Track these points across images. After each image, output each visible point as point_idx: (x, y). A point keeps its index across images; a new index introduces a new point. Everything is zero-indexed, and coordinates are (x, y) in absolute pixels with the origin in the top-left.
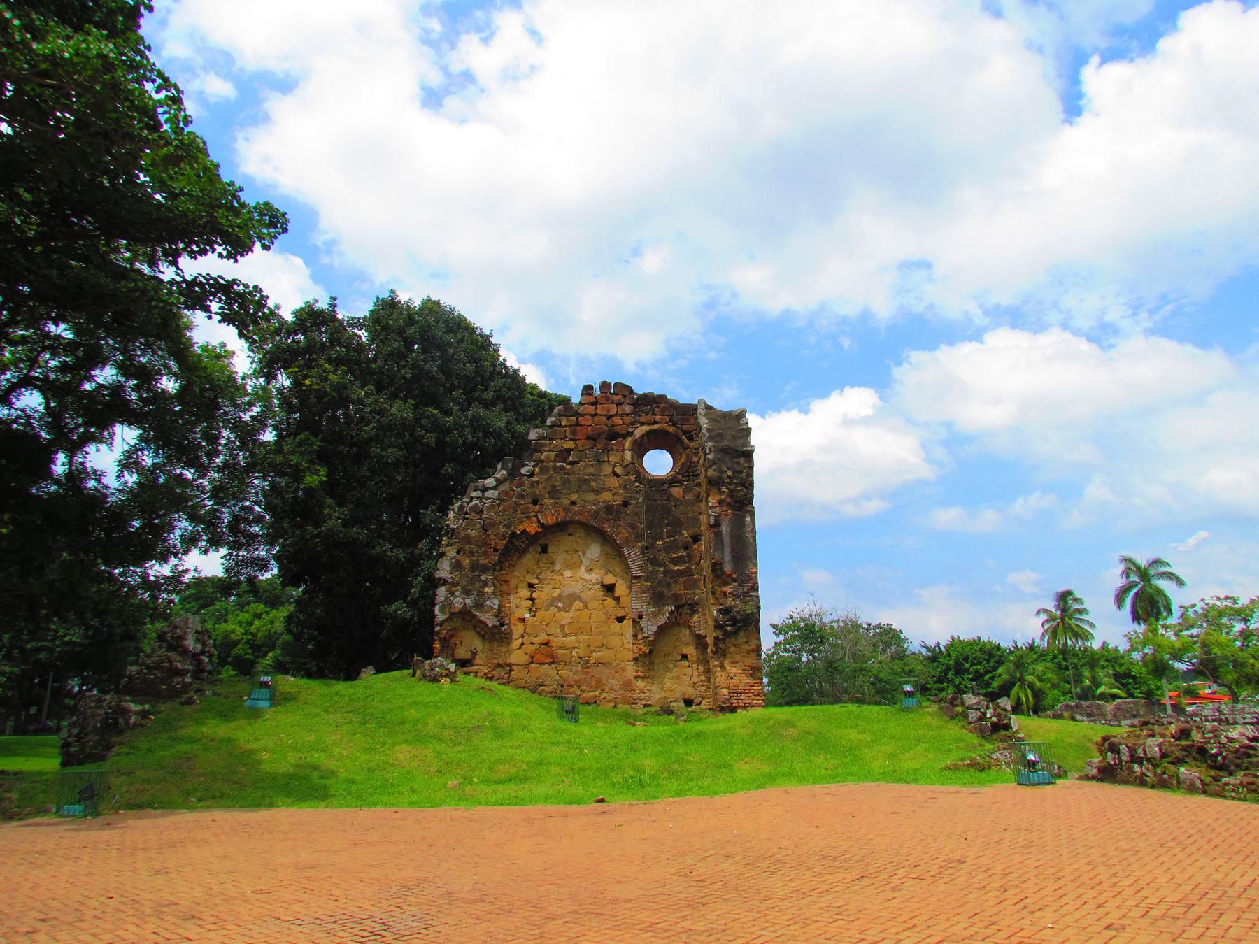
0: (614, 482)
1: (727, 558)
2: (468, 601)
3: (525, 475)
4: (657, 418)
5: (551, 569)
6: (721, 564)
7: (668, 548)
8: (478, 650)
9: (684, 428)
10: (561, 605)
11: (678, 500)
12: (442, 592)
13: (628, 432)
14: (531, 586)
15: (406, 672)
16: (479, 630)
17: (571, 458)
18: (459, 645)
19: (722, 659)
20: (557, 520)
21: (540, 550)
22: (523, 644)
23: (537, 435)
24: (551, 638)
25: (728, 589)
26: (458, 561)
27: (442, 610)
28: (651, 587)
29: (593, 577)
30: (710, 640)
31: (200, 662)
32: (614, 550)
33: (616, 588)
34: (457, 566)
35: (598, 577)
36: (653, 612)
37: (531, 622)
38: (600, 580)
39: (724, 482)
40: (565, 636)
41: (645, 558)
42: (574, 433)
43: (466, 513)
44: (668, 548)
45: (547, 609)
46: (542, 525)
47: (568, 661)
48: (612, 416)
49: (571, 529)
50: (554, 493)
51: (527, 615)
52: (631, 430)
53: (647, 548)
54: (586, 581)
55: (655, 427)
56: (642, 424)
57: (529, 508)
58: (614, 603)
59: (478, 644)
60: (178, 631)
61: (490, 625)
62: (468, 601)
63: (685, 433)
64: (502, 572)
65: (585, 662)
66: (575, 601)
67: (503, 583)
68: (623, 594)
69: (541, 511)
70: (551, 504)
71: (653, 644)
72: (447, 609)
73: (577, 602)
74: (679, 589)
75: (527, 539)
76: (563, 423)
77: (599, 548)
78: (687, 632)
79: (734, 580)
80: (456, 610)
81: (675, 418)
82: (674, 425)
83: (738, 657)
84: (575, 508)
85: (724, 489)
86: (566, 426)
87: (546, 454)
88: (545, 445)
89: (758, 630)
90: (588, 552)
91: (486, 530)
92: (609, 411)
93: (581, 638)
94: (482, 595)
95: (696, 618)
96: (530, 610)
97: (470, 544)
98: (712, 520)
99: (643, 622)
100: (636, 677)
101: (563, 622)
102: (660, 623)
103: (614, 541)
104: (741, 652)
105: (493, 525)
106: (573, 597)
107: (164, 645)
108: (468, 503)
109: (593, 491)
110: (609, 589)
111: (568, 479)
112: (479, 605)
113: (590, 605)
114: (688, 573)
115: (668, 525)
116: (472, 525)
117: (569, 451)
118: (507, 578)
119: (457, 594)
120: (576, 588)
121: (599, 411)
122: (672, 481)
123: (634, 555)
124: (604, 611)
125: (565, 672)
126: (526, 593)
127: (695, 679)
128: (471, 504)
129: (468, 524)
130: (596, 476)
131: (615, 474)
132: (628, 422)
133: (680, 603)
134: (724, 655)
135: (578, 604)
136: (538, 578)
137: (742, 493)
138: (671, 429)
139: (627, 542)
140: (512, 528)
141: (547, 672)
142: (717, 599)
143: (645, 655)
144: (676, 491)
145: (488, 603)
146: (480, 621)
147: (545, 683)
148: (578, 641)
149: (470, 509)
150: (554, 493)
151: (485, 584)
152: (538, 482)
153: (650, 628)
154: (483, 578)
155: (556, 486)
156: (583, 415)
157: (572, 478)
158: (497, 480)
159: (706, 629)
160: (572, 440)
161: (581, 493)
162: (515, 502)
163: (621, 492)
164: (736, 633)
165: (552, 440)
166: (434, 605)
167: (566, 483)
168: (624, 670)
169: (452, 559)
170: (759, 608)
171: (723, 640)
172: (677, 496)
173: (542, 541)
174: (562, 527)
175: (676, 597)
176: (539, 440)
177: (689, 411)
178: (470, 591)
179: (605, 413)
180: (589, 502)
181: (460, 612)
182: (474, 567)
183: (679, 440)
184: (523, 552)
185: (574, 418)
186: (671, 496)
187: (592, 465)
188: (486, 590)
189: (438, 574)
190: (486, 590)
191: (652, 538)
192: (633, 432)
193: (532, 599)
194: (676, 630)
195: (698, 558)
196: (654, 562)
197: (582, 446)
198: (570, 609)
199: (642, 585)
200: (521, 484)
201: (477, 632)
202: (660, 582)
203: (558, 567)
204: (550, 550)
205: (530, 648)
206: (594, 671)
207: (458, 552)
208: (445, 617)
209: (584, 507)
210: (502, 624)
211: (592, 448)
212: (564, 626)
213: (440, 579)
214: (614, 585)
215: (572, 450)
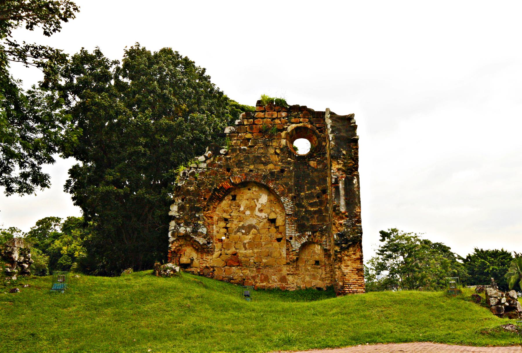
0: (276, 158)
1: (342, 202)
2: (188, 229)
3: (223, 154)
4: (301, 120)
5: (238, 210)
6: (339, 206)
8: (194, 258)
10: (244, 231)
12: (173, 224)
13: (284, 128)
14: (226, 220)
15: (150, 271)
16: (195, 246)
17: (250, 144)
18: (183, 255)
19: (340, 264)
20: (241, 180)
21: (231, 198)
22: (221, 255)
23: (230, 130)
24: (238, 251)
25: (342, 221)
26: (182, 205)
27: (173, 235)
28: (298, 220)
29: (263, 215)
30: (332, 252)
31: (23, 267)
33: (277, 221)
34: (181, 208)
35: (266, 215)
36: (298, 236)
37: (225, 241)
38: (267, 217)
39: (340, 158)
41: (294, 203)
42: (251, 129)
43: (187, 177)
45: (236, 233)
46: (233, 184)
47: (248, 265)
49: (250, 187)
50: (239, 164)
51: (224, 238)
52: (286, 127)
53: (295, 197)
54: (259, 217)
55: (301, 125)
56: (293, 123)
57: (224, 173)
58: (275, 230)
59: (194, 255)
60: (8, 248)
61: (201, 243)
63: (318, 128)
64: (209, 212)
66: (252, 229)
67: (209, 218)
68: (281, 224)
69: (231, 175)
70: (238, 171)
71: (298, 254)
72: (176, 234)
74: (314, 222)
75: (223, 191)
76: (245, 123)
77: (267, 197)
79: (347, 216)
80: (181, 235)
81: (312, 119)
82: (311, 124)
83: (349, 263)
85: (340, 162)
86: (247, 125)
87: (235, 141)
88: (235, 136)
89: (361, 247)
90: (260, 200)
91: (199, 187)
92: (272, 115)
93: (256, 251)
95: (324, 238)
96: (225, 234)
97: (190, 195)
98: (333, 180)
99: (293, 242)
100: (288, 274)
101: (245, 242)
102: (302, 242)
103: (276, 193)
104: (351, 260)
105: (203, 183)
106: (251, 227)
108: (188, 171)
111: (248, 156)
112: (195, 232)
113: (261, 232)
114: (320, 212)
115: (307, 183)
116: (190, 183)
117: (249, 140)
118: (212, 215)
119: (182, 225)
120: (254, 222)
121: (266, 116)
122: (310, 156)
123: (287, 201)
124: (269, 235)
125: (247, 272)
126: (222, 224)
127: (323, 276)
128: (191, 171)
129: (188, 183)
130: (265, 156)
131: (276, 153)
132: (284, 122)
133: (315, 230)
135: (254, 231)
136: (230, 215)
137: (351, 164)
138: (309, 126)
139: (283, 194)
140: (215, 186)
141: (236, 272)
143: (294, 261)
144: (312, 163)
145: (200, 230)
146: (195, 241)
147: (234, 278)
148: (254, 253)
149: (189, 175)
151: (199, 219)
152: (230, 158)
153: (296, 245)
154: (197, 215)
155: (241, 161)
156: (257, 118)
159: (330, 245)
160: (250, 133)
161: (256, 164)
162: (217, 170)
163: (279, 163)
164: (347, 248)
165: (238, 133)
166: (168, 231)
167: (247, 158)
168: (281, 270)
169: (179, 204)
170: (361, 233)
171: (340, 252)
172: (313, 166)
173: (232, 193)
174: (245, 184)
176: (231, 133)
177: (321, 115)
178: (190, 223)
179: (270, 117)
180: (260, 170)
181: (183, 236)
182: (192, 208)
183: (314, 132)
184: (221, 200)
185: (252, 120)
186: (310, 166)
187: (262, 148)
188: (199, 222)
189: (170, 214)
190: (199, 222)
191: (298, 191)
192: (287, 128)
194: (312, 247)
195: (326, 203)
196: (299, 205)
197: (257, 136)
198: (249, 233)
199: (292, 219)
200: (220, 159)
201: (194, 248)
202: (303, 217)
203: (242, 209)
204: (236, 199)
205: (224, 257)
206: (264, 271)
207: (183, 200)
208: (175, 239)
209: (258, 173)
210: (209, 243)
211: (262, 138)
212: (246, 244)
213: (171, 216)
215: (250, 139)
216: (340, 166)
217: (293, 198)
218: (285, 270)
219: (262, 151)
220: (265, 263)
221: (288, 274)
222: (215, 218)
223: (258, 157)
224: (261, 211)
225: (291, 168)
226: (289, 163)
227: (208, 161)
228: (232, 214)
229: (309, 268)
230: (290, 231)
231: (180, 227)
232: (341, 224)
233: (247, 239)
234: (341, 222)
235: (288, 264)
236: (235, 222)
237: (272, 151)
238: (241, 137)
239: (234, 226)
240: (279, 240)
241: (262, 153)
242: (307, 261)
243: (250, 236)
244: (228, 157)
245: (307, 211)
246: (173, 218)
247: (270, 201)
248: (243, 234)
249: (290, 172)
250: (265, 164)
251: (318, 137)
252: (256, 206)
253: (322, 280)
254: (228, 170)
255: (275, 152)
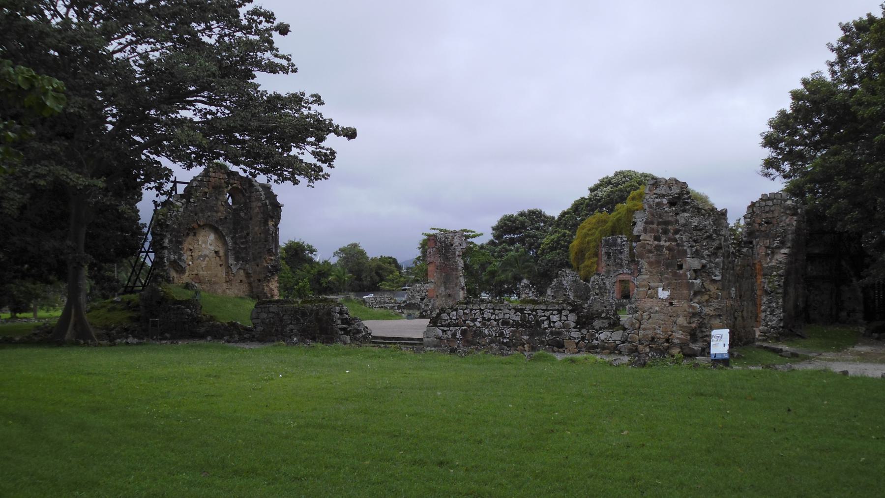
0: (222, 208)
2: (176, 257)
4: (236, 182)
7: (240, 237)
9: (245, 187)
10: (202, 259)
11: (242, 218)
12: (166, 251)
19: (267, 283)
21: (193, 234)
25: (272, 258)
26: (171, 239)
28: (235, 253)
29: (212, 248)
32: (220, 236)
34: (170, 241)
35: (214, 248)
40: (203, 272)
42: (208, 185)
44: (240, 237)
46: (199, 226)
48: (220, 179)
51: (190, 263)
62: (176, 257)
65: (210, 282)
73: (207, 258)
76: (204, 180)
78: (242, 271)
79: (274, 255)
83: (273, 283)
84: (210, 219)
88: (198, 189)
91: (180, 226)
92: (220, 176)
93: (209, 272)
94: (180, 255)
95: (247, 266)
100: (226, 289)
101: (203, 266)
106: (206, 256)
107: (164, 280)
109: (215, 211)
110: (217, 252)
112: (180, 259)
116: (174, 223)
117: (206, 193)
119: (172, 253)
120: (207, 252)
121: (216, 176)
123: (228, 239)
126: (189, 253)
127: (244, 290)
128: (174, 214)
131: (222, 205)
134: (269, 281)
138: (240, 187)
139: (227, 235)
142: (266, 261)
145: (182, 258)
146: (180, 265)
150: (202, 211)
154: (180, 247)
157: (208, 205)
158: (182, 204)
175: (243, 258)
183: (241, 192)
184: (188, 234)
190: (181, 252)
193: (191, 256)
196: (235, 243)
200: (191, 207)
201: (174, 269)
213: (165, 247)
214: (218, 251)
215: (207, 192)
216: (274, 223)
217: (232, 238)
218: (225, 285)
219: (215, 202)
220: (214, 281)
221: (226, 289)
222: (185, 249)
223: (213, 207)
224: (211, 245)
225: (231, 217)
226: (229, 213)
227: (183, 207)
228: (195, 246)
229: (237, 284)
230: (231, 261)
231: (171, 255)
232: (272, 259)
233: (204, 264)
234: (272, 258)
235: (227, 282)
236: (196, 252)
237: (220, 203)
238: (202, 190)
239: (196, 255)
240: (221, 265)
241: (215, 204)
242: (236, 280)
243: (205, 262)
244: (195, 205)
245: (240, 247)
246: (165, 248)
247: (215, 238)
248: (201, 261)
249: (230, 219)
250: (217, 212)
251: (244, 195)
252: (208, 241)
253: (244, 292)
254: (196, 215)
255: (222, 204)
